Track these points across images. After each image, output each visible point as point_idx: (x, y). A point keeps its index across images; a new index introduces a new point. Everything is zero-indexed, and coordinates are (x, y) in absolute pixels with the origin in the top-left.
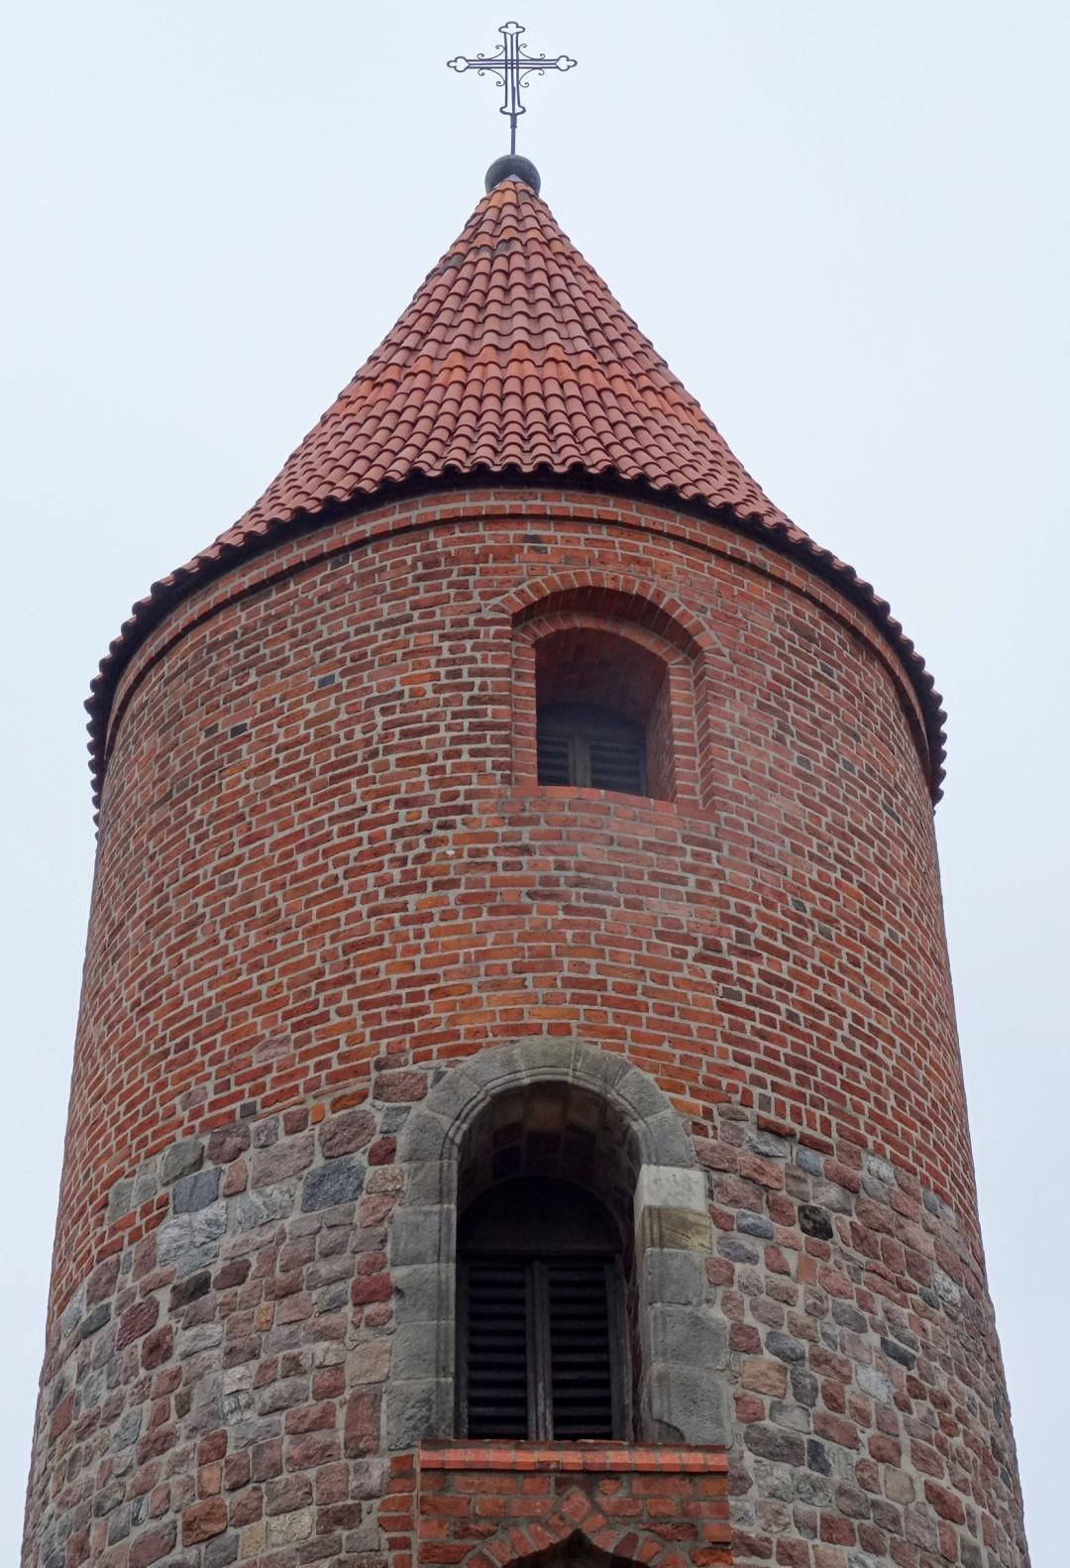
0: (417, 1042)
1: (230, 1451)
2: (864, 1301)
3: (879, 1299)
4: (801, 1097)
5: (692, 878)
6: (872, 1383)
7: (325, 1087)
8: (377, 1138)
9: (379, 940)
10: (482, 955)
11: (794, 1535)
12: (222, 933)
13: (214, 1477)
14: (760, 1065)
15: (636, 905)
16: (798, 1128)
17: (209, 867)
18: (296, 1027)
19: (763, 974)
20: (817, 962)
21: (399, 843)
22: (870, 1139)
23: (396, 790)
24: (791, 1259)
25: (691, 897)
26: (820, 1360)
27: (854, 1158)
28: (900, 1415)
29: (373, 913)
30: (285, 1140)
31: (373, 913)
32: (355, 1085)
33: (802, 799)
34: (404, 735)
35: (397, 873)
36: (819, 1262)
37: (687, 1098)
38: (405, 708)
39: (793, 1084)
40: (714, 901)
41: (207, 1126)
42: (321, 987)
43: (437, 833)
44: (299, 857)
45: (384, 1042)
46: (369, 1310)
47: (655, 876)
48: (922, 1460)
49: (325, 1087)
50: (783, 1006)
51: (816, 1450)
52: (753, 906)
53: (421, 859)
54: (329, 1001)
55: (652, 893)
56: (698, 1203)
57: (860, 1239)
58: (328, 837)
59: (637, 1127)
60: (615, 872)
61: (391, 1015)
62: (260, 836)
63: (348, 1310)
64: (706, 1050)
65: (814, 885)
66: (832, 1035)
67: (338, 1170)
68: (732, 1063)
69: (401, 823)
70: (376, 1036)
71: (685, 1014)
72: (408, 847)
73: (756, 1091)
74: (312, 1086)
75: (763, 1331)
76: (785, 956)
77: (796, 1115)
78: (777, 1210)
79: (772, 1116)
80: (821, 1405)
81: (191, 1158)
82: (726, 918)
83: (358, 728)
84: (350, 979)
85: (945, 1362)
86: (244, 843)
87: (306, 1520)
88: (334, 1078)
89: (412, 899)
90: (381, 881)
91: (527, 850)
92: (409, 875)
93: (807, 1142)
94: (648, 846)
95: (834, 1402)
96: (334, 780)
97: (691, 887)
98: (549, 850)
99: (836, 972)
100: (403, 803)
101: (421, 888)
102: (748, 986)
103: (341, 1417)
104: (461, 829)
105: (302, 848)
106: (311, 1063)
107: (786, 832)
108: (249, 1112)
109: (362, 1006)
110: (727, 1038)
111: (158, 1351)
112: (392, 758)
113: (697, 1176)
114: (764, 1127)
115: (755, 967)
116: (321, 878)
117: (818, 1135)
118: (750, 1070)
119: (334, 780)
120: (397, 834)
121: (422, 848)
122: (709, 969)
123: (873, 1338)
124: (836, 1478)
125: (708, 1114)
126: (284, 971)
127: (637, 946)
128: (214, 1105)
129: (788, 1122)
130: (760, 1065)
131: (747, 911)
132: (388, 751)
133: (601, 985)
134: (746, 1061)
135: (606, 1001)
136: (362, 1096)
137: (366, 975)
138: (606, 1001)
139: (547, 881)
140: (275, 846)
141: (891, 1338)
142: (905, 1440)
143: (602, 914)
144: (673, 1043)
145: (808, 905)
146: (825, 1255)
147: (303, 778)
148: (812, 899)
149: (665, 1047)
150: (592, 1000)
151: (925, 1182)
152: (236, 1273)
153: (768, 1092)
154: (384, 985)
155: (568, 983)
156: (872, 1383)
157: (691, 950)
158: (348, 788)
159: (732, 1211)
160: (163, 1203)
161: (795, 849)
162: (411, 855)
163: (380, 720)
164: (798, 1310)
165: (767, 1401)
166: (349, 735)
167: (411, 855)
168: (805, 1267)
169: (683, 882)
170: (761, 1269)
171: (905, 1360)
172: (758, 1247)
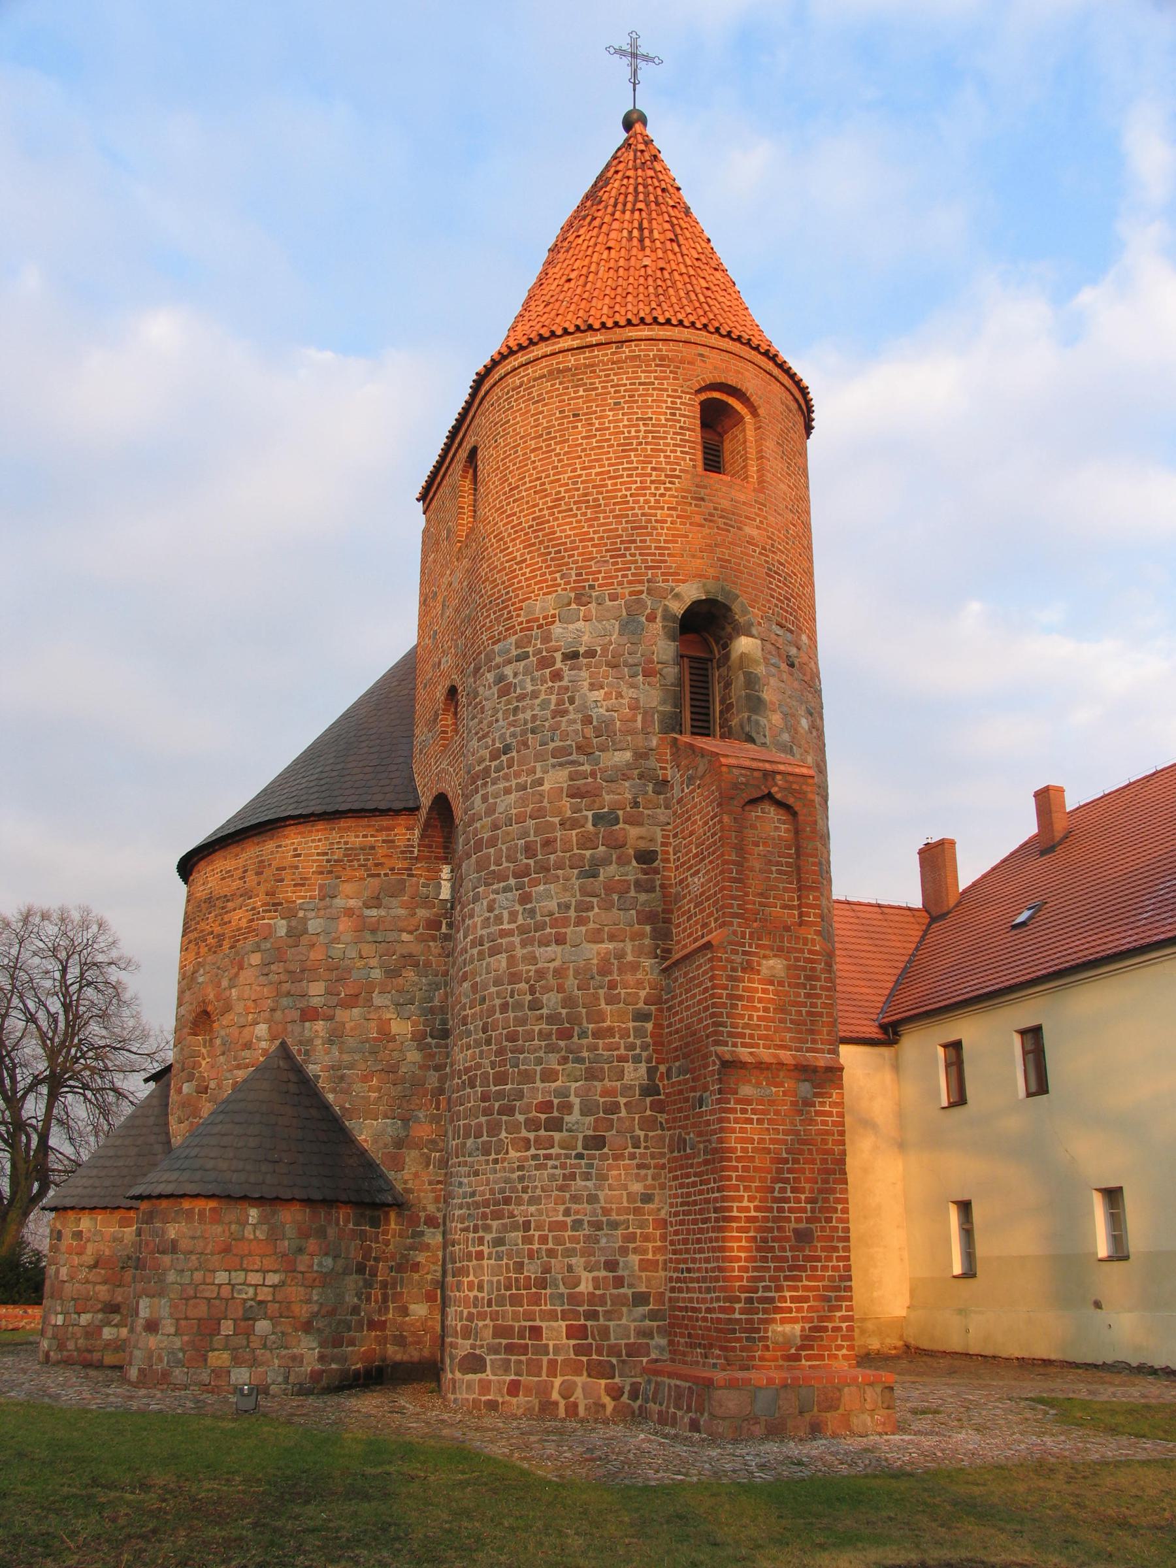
0: (663, 574)
1: (595, 723)
7: (626, 585)
8: (649, 611)
9: (646, 528)
12: (575, 507)
13: (589, 732)
17: (566, 476)
18: (611, 557)
21: (653, 486)
23: (651, 463)
29: (643, 515)
30: (608, 603)
31: (643, 515)
32: (639, 588)
34: (653, 437)
35: (652, 499)
38: (653, 425)
41: (572, 589)
42: (622, 542)
43: (668, 485)
44: (609, 482)
45: (650, 572)
46: (648, 679)
49: (626, 585)
53: (662, 495)
54: (626, 549)
56: (758, 654)
58: (621, 476)
61: (652, 561)
62: (591, 468)
63: (640, 678)
67: (633, 621)
69: (653, 478)
70: (647, 568)
72: (657, 489)
74: (620, 584)
81: (566, 601)
83: (633, 430)
84: (634, 542)
86: (583, 469)
87: (628, 755)
88: (630, 582)
89: (659, 512)
90: (647, 502)
92: (657, 501)
96: (623, 451)
100: (653, 469)
101: (662, 508)
103: (639, 718)
104: (678, 485)
105: (610, 478)
106: (620, 574)
108: (592, 587)
109: (641, 554)
111: (557, 676)
112: (649, 447)
116: (619, 494)
119: (623, 451)
120: (652, 482)
121: (662, 491)
126: (604, 531)
128: (575, 582)
132: (647, 443)
136: (642, 592)
137: (641, 541)
139: (711, 515)
140: (597, 474)
147: (609, 447)
152: (591, 653)
154: (649, 548)
158: (630, 456)
160: (553, 616)
162: (658, 492)
163: (642, 428)
166: (629, 432)
167: (658, 492)
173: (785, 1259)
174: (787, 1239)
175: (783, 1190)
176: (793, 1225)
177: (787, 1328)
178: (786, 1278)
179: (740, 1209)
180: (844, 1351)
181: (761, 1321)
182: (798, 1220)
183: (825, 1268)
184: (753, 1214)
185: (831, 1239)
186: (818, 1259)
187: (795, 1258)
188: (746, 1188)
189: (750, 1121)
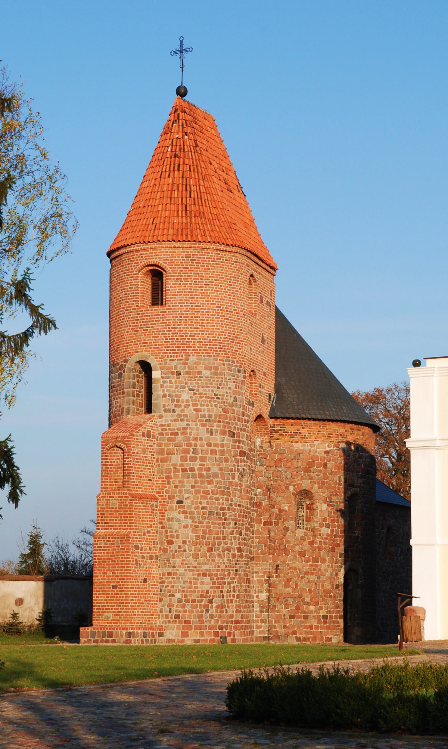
2: (186, 383)
3: (189, 382)
4: (178, 353)
5: (161, 319)
6: (185, 396)
10: (134, 339)
11: (169, 422)
14: (171, 350)
15: (152, 327)
16: (177, 359)
19: (172, 333)
20: (184, 326)
22: (191, 355)
24: (173, 381)
25: (161, 323)
26: (176, 396)
27: (188, 359)
28: (190, 399)
33: (184, 295)
36: (178, 380)
37: (159, 359)
39: (176, 351)
40: (164, 323)
47: (156, 321)
48: (194, 405)
50: (176, 338)
51: (174, 410)
52: (171, 321)
55: (155, 324)
57: (187, 373)
59: (152, 365)
60: (150, 321)
64: (162, 350)
65: (185, 311)
66: (185, 339)
68: (166, 351)
71: (159, 345)
73: (169, 355)
75: (167, 394)
76: (177, 328)
77: (177, 357)
78: (173, 373)
79: (172, 358)
80: (175, 403)
82: (166, 325)
85: (203, 387)
91: (138, 320)
93: (178, 360)
94: (155, 315)
95: (178, 401)
97: (161, 321)
98: (141, 319)
99: (188, 326)
102: (169, 337)
107: (179, 303)
110: (165, 347)
113: (159, 372)
114: (170, 360)
115: (171, 332)
117: (181, 358)
118: (169, 351)
122: (163, 336)
123: (187, 389)
124: (176, 413)
125: (162, 361)
127: (152, 334)
129: (175, 358)
130: (171, 350)
131: (170, 323)
133: (147, 343)
134: (168, 350)
135: (148, 346)
138: (148, 346)
141: (191, 388)
142: (191, 403)
143: (147, 330)
144: (158, 351)
145: (183, 316)
146: (179, 378)
148: (183, 314)
149: (156, 352)
150: (145, 346)
151: (205, 356)
153: (172, 354)
155: (143, 343)
156: (185, 396)
157: (160, 333)
159: (165, 376)
161: (181, 306)
164: (174, 389)
165: (167, 404)
168: (176, 381)
169: (160, 321)
170: (168, 384)
171: (193, 390)
172: (168, 380)
173: (109, 594)
174: (110, 588)
175: (110, 573)
176: (112, 584)
177: (109, 614)
178: (109, 600)
179: (97, 580)
180: (124, 622)
181: (102, 612)
182: (114, 582)
183: (120, 597)
184: (101, 581)
185: (122, 588)
186: (118, 594)
187: (112, 594)
188: (100, 573)
189: (101, 553)
